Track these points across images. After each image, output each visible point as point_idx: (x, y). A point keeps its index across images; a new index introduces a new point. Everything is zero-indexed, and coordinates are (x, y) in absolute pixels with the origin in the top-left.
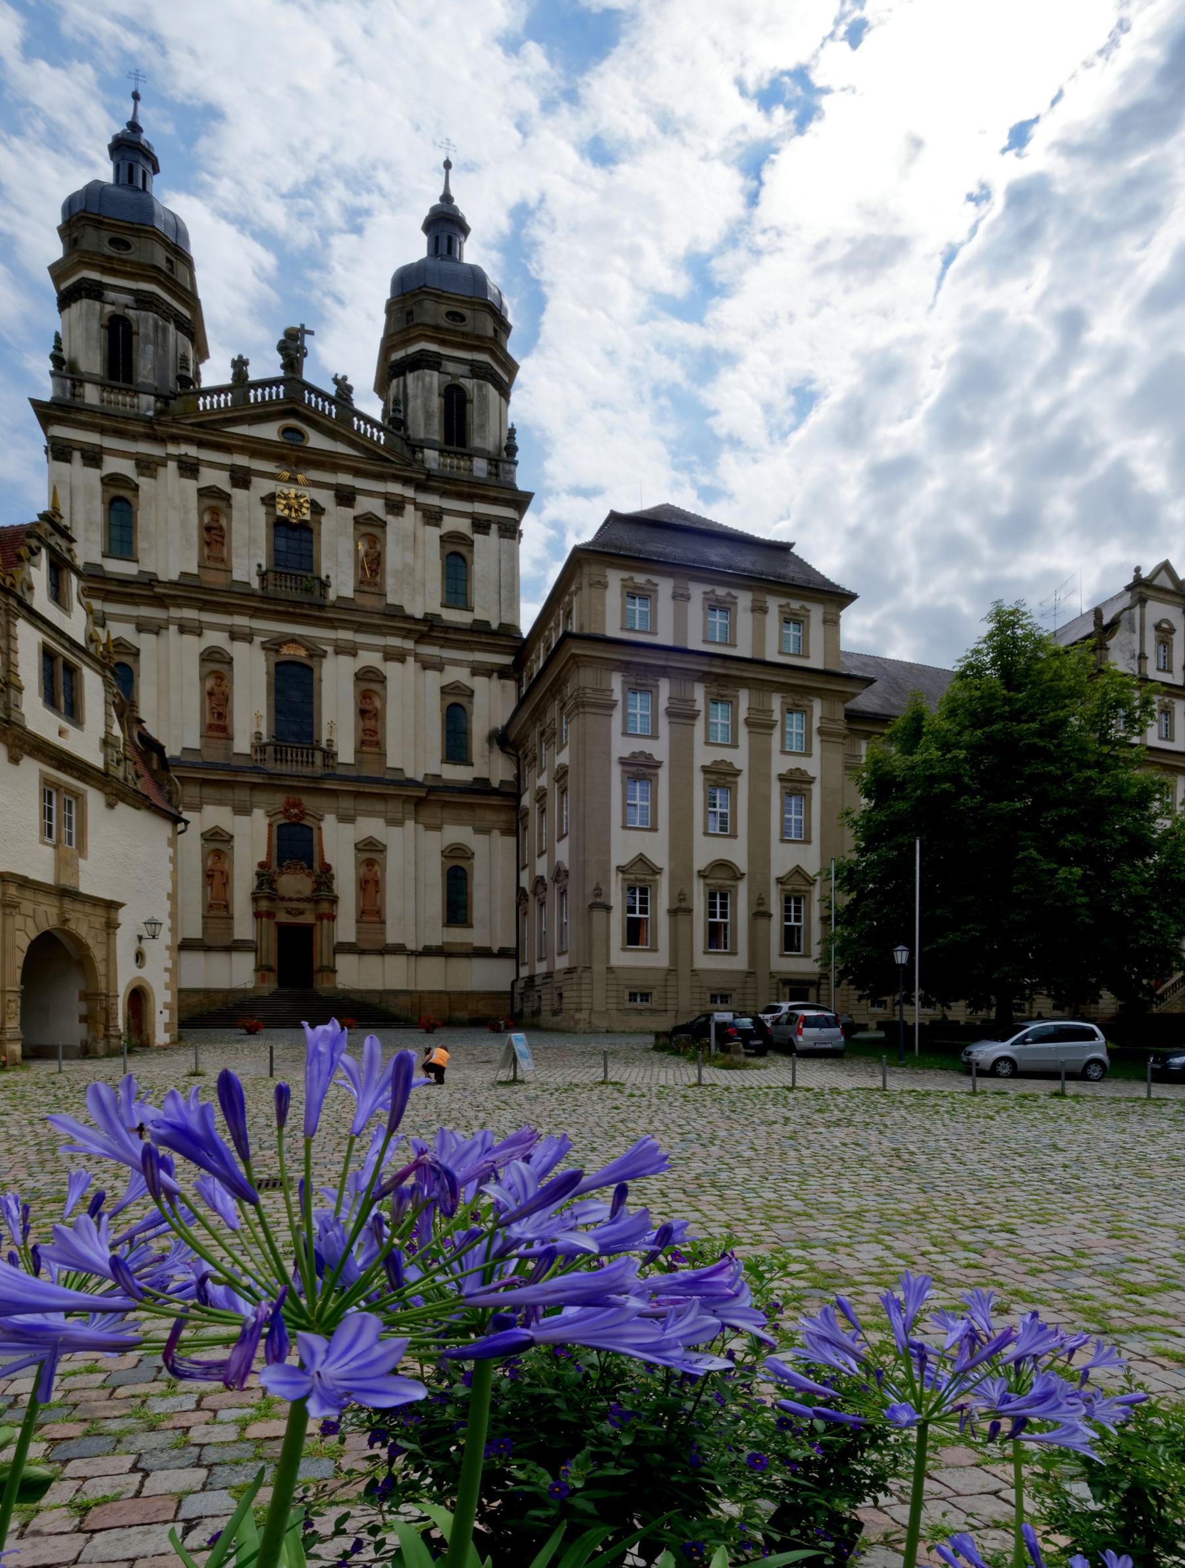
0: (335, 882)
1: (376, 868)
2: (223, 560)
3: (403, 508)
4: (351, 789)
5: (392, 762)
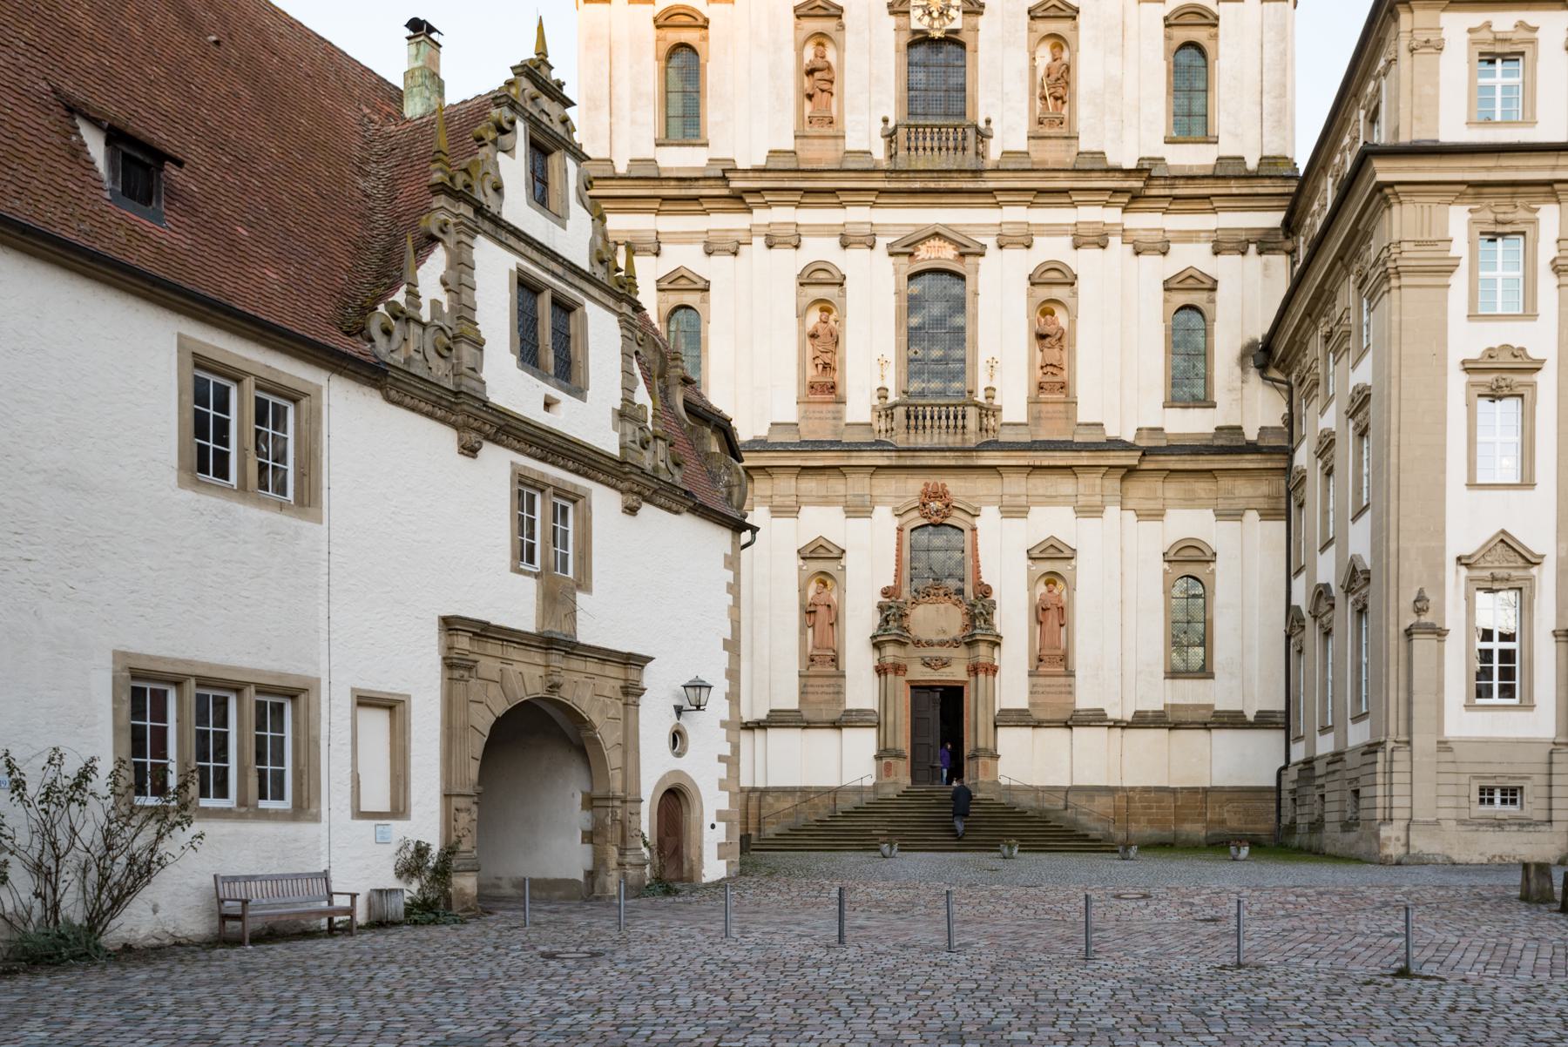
0: (997, 613)
1: (1060, 585)
5: (1083, 416)
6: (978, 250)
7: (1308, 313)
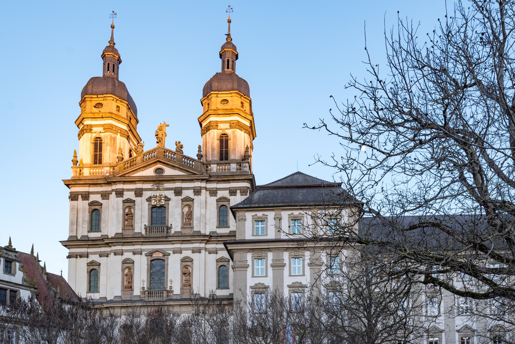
3: (201, 192)
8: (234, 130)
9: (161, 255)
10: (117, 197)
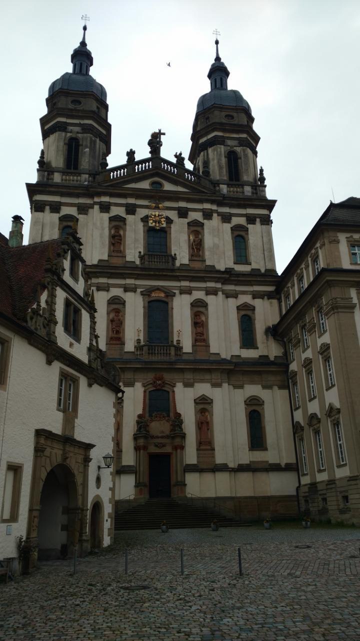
0: (183, 425)
1: (207, 414)
2: (121, 251)
3: (212, 215)
4: (192, 367)
6: (173, 294)
7: (294, 318)
8: (245, 148)
9: (162, 295)
10: (101, 212)
